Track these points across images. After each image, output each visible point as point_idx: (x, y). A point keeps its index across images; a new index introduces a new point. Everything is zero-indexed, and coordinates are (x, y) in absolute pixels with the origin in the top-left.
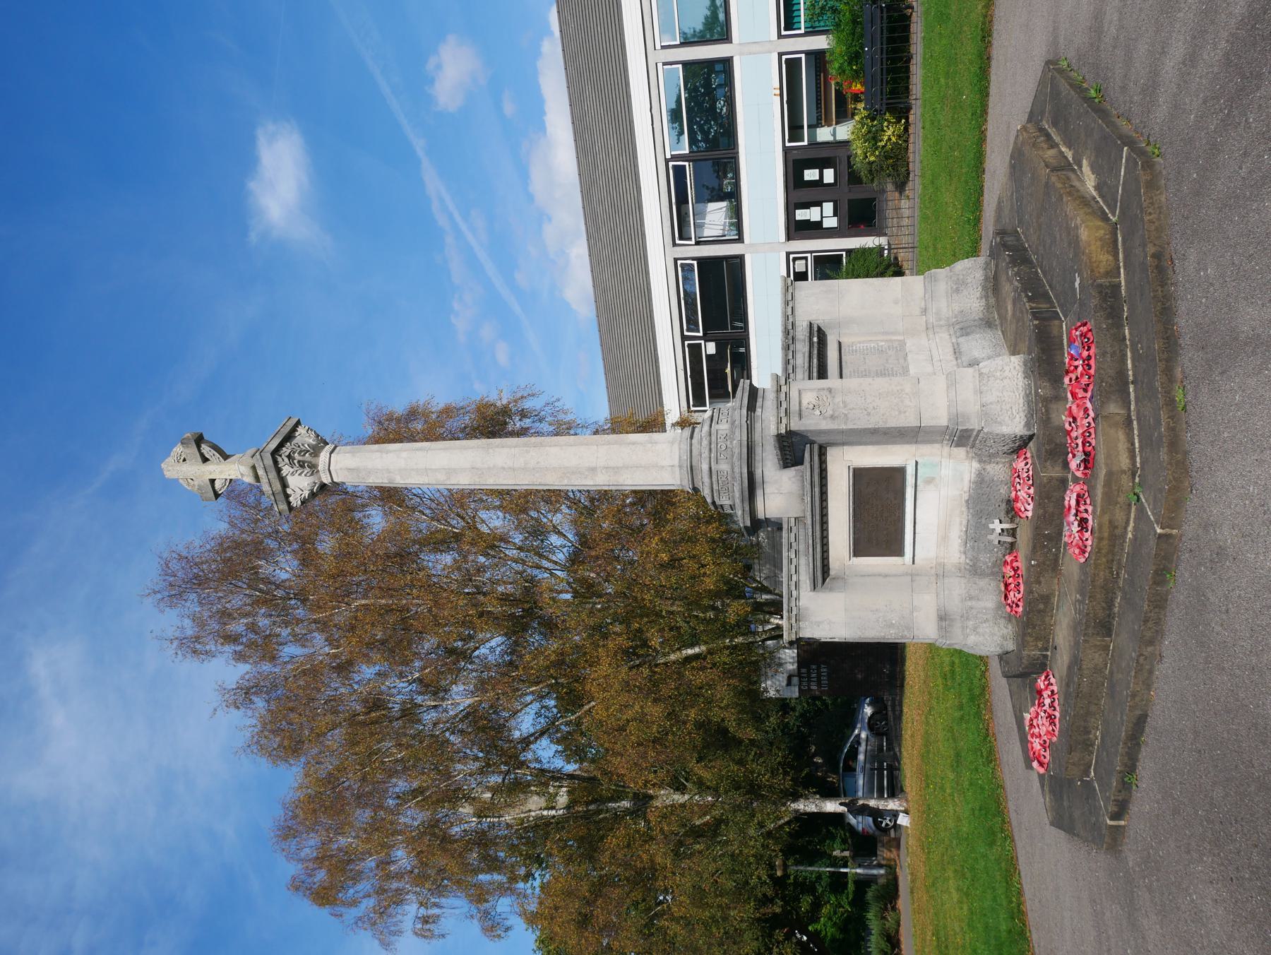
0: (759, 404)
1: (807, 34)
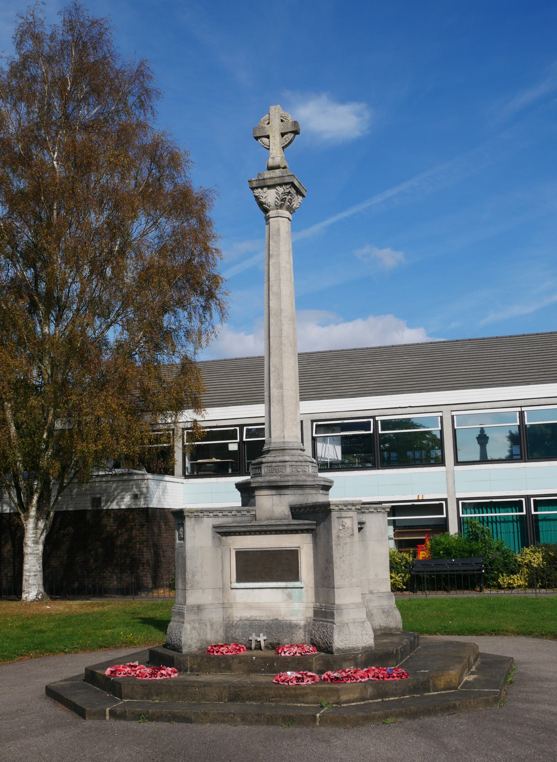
1: (459, 518)
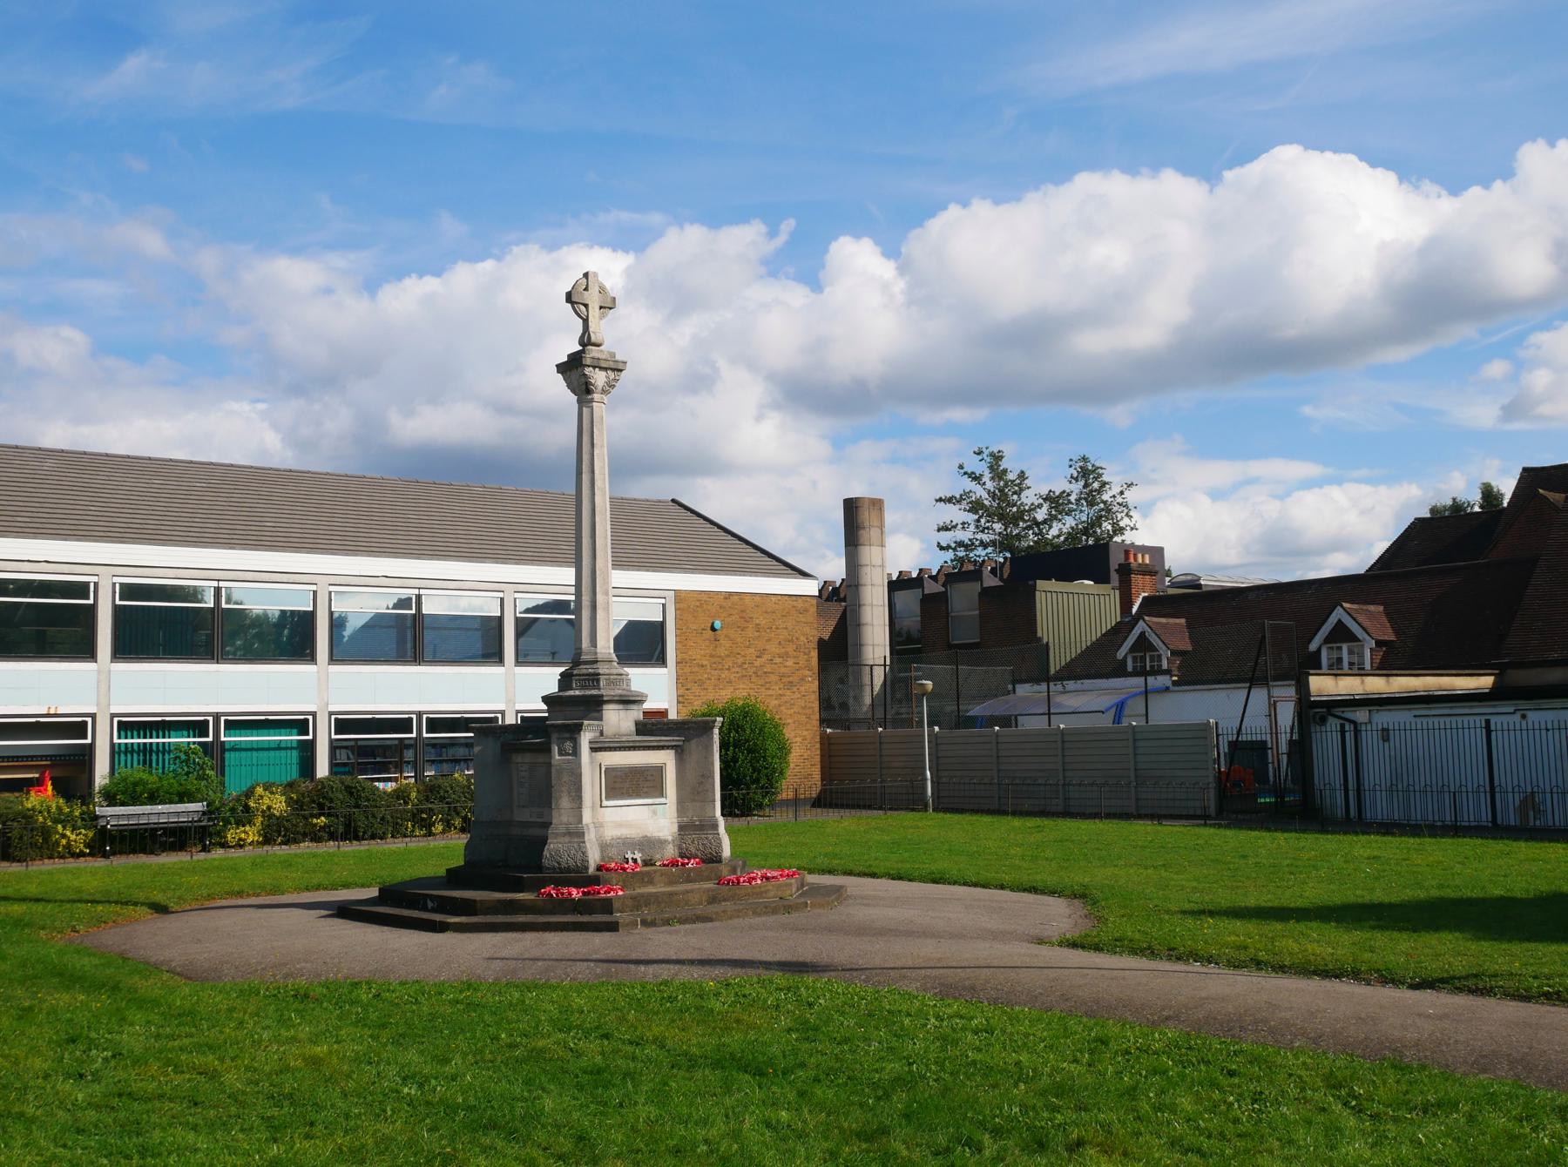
1: (112, 745)
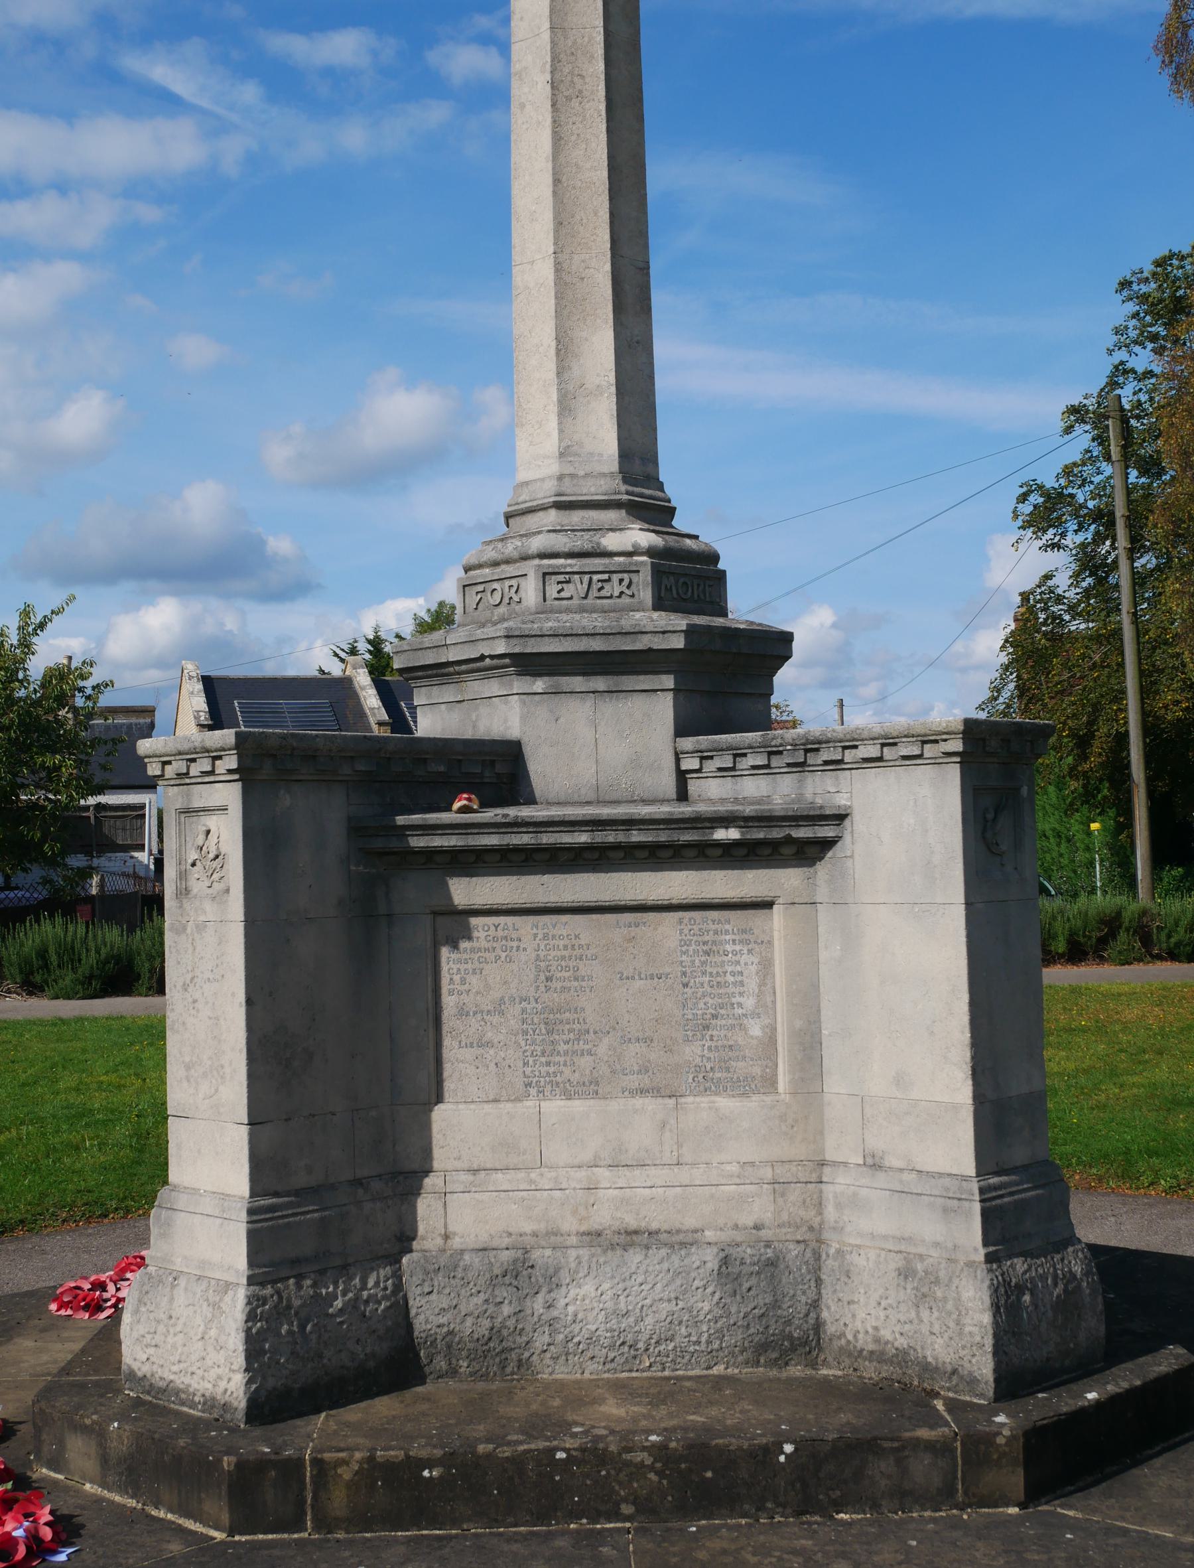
0: (600, 683)
